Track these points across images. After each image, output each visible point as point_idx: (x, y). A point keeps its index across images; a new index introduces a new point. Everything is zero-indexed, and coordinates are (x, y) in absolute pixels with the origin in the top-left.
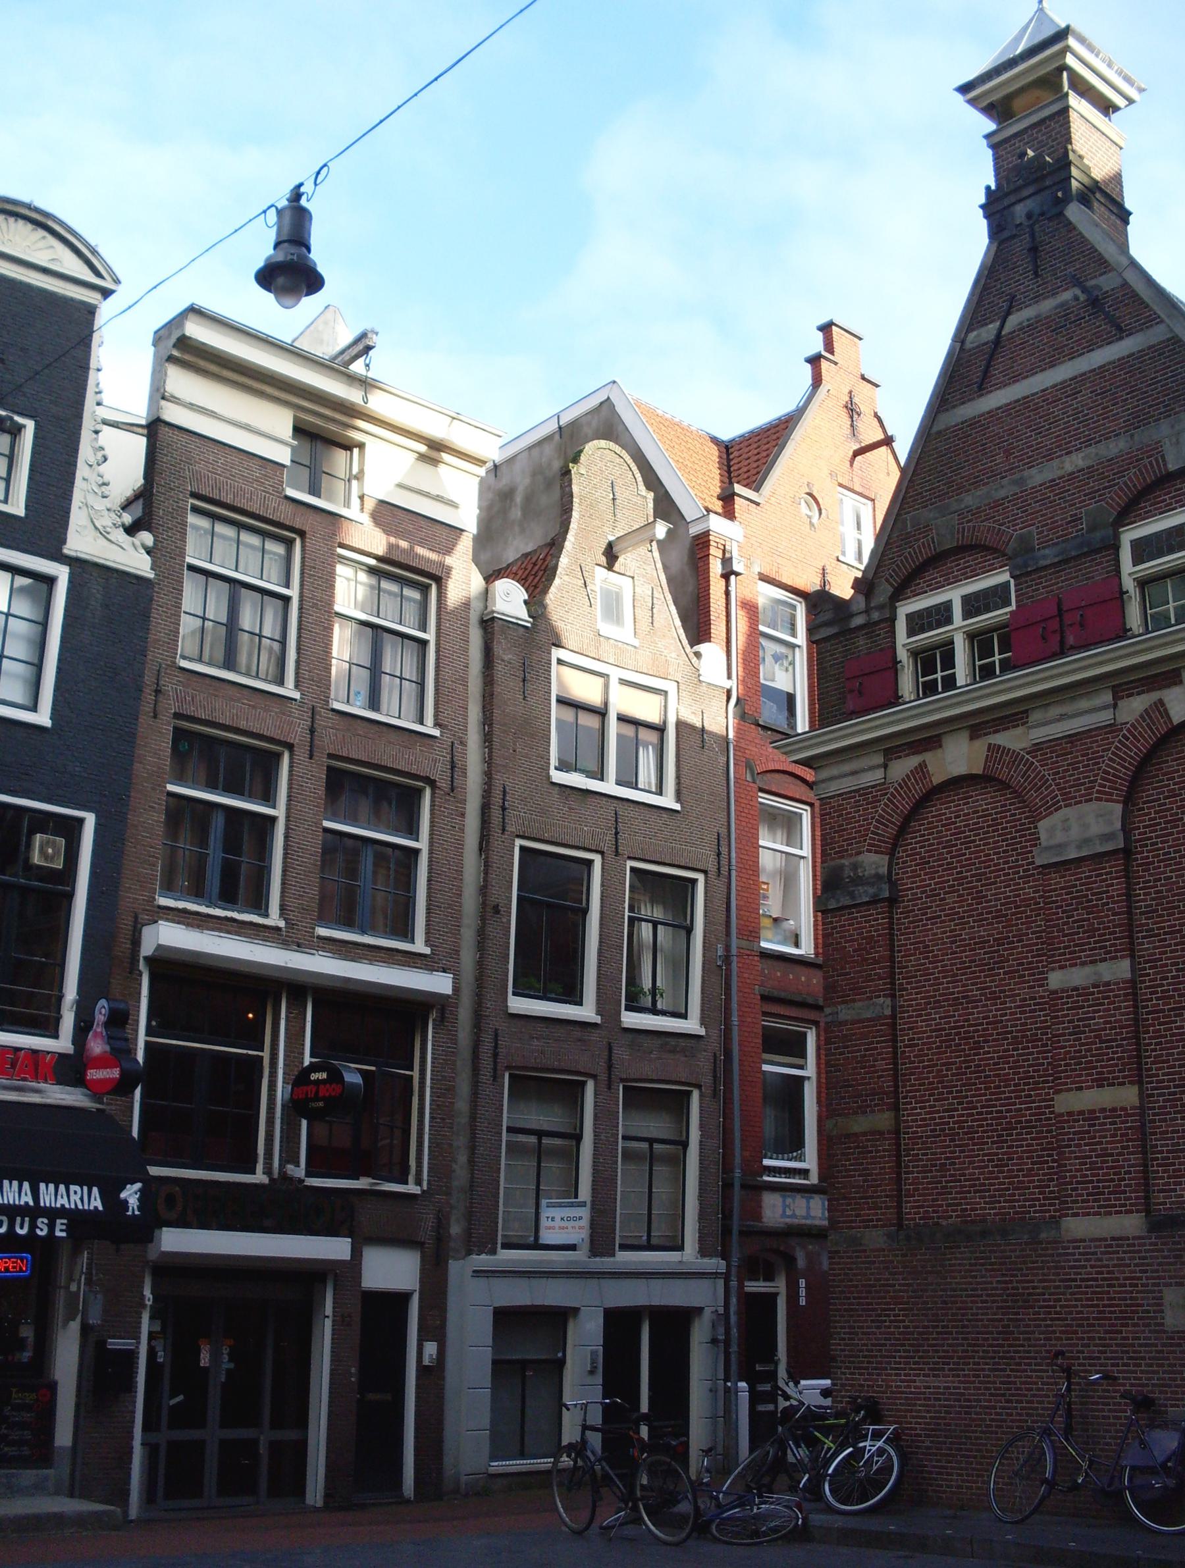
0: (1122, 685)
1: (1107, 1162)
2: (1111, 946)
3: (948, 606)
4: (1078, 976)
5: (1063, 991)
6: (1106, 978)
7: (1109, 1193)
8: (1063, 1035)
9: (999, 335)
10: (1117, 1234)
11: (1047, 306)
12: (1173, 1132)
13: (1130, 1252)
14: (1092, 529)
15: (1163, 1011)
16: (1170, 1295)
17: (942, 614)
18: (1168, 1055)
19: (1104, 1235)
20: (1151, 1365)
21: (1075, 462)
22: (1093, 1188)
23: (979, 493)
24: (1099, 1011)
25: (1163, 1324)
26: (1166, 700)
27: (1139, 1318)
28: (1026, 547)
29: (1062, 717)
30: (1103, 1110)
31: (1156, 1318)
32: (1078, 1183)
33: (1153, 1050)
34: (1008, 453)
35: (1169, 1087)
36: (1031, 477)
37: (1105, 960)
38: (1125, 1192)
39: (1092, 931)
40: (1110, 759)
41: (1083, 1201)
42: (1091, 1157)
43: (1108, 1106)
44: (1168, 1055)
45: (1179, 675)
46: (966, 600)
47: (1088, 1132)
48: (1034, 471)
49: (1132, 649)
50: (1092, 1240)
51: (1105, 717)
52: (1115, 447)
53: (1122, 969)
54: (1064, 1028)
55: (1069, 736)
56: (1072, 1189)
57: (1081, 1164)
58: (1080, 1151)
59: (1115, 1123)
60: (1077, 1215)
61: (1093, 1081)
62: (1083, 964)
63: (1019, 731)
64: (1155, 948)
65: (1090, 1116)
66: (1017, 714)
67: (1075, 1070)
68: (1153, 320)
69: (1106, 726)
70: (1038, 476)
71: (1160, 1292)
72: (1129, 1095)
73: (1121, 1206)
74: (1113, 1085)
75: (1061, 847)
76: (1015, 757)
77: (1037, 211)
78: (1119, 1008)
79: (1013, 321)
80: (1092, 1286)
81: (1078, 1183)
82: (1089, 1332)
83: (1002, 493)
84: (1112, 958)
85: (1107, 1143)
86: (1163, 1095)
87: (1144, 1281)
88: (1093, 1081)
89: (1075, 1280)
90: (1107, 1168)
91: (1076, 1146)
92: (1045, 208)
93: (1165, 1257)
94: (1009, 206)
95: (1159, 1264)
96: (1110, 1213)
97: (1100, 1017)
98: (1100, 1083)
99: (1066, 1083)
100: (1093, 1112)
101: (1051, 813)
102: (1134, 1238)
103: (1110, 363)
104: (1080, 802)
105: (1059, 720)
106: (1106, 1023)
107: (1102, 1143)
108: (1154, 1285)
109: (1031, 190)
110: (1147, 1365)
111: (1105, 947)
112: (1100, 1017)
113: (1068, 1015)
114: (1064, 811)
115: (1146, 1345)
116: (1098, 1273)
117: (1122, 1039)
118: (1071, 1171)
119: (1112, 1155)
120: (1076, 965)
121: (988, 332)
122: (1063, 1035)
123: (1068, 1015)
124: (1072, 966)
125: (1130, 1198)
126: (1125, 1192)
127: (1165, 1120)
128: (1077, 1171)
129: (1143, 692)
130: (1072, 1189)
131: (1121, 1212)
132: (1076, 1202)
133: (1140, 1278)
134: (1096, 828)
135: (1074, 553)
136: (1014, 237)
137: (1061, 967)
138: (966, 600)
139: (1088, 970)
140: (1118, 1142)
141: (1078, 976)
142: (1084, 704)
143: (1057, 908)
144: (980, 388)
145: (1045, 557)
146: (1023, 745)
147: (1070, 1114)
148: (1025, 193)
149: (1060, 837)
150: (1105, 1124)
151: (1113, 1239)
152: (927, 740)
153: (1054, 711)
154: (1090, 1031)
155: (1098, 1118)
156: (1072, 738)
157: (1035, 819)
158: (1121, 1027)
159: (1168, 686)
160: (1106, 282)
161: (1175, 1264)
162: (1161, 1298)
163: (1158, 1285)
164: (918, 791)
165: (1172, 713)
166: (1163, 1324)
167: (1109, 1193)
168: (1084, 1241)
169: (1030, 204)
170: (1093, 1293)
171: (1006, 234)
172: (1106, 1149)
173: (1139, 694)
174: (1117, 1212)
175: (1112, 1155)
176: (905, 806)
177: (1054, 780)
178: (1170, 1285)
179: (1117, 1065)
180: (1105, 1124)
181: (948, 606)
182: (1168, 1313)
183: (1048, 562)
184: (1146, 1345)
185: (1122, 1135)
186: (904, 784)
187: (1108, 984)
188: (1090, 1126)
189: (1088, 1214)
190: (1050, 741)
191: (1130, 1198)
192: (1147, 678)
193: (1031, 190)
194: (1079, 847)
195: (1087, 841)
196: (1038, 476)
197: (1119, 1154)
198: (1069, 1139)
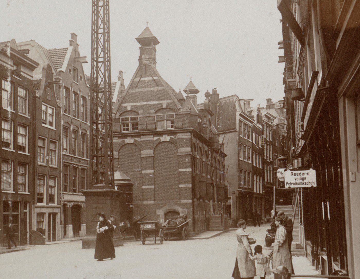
3: (128, 118)
9: (139, 80)
17: (127, 119)
46: (131, 118)
51: (152, 139)
63: (139, 139)
68: (162, 86)
72: (153, 187)
76: (138, 142)
79: (142, 79)
121: (137, 80)
138: (131, 118)
144: (136, 88)
157: (141, 150)
164: (123, 144)
176: (121, 145)
181: (128, 118)
186: (121, 142)
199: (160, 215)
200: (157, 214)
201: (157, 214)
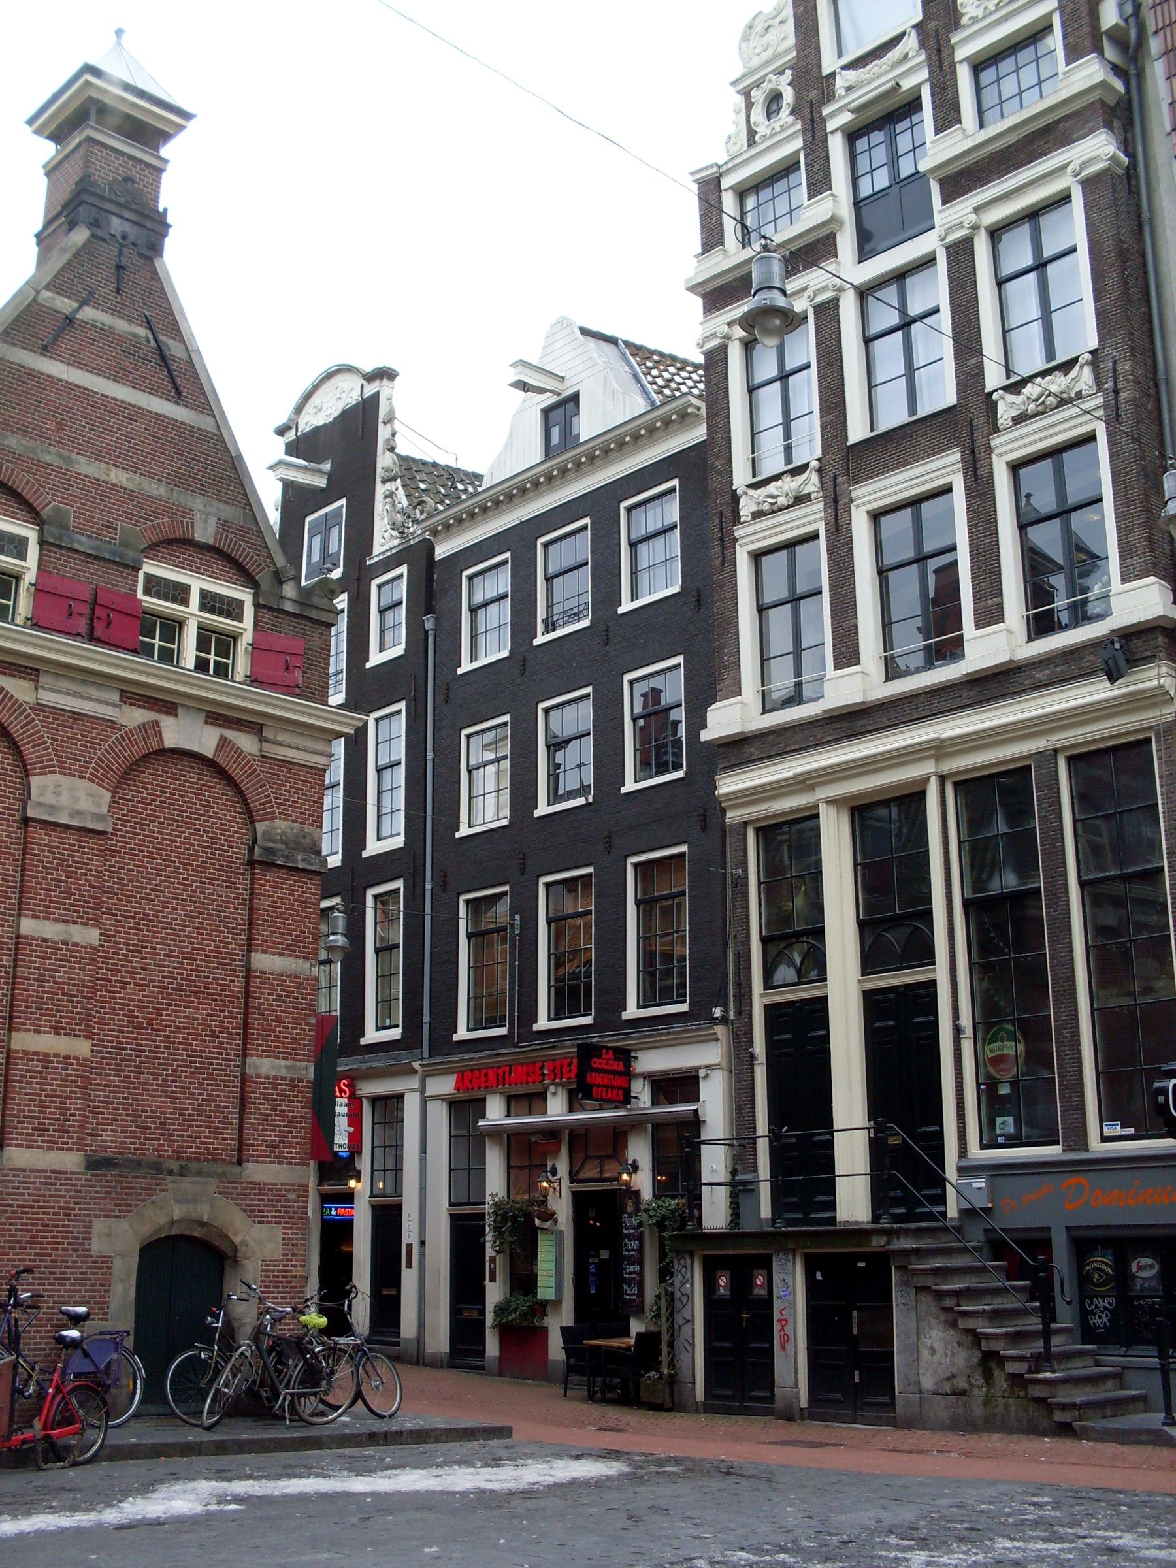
0: (132, 694)
1: (55, 1102)
2: (85, 912)
4: (50, 930)
5: (33, 938)
6: (76, 940)
7: (54, 1131)
8: (29, 979)
10: (57, 1167)
11: (121, 325)
12: (106, 1086)
13: (67, 1185)
14: (125, 544)
15: (111, 981)
16: (99, 1225)
18: (110, 1019)
19: (44, 1168)
20: (75, 1285)
21: (119, 477)
22: (39, 1124)
23: (24, 442)
24: (64, 966)
25: (89, 1250)
26: (162, 724)
27: (69, 1244)
28: (60, 521)
29: (76, 695)
30: (57, 1055)
31: (83, 1244)
32: (25, 1117)
33: (97, 1012)
34: (60, 426)
35: (107, 1047)
36: (77, 462)
37: (75, 923)
38: (68, 1132)
39: (68, 894)
40: (106, 750)
41: (28, 1134)
42: (41, 1095)
43: (63, 1053)
44: (110, 1019)
45: (176, 710)
47: (41, 1072)
48: (82, 459)
49: (156, 672)
50: (32, 1171)
52: (157, 489)
53: (28, 926)
54: (29, 973)
55: (74, 713)
56: (19, 1122)
57: (30, 1100)
58: (31, 1088)
59: (67, 1069)
60: (20, 1146)
61: (51, 1027)
62: (56, 920)
64: (112, 925)
65: (45, 1058)
66: (26, 667)
67: (35, 1014)
69: (108, 720)
70: (85, 466)
71: (91, 1222)
73: (63, 1143)
74: (69, 1035)
75: (53, 808)
77: (131, 238)
78: (84, 969)
79: (88, 313)
80: (28, 1213)
81: (25, 1117)
82: (20, 1254)
83: (48, 458)
84: (82, 924)
85: (58, 1085)
86: (101, 1052)
87: (77, 1211)
88: (51, 1027)
89: (12, 1206)
90: (55, 1108)
91: (27, 1083)
92: (139, 242)
93: (97, 1192)
94: (107, 211)
95: (91, 1198)
96: (52, 1149)
97: (65, 972)
98: (57, 1030)
99: (25, 1024)
100: (47, 1055)
101: (45, 773)
102: (72, 1173)
103: (165, 416)
104: (74, 776)
105: (69, 695)
106: (69, 978)
107: (52, 1085)
108: (85, 1215)
109: (132, 217)
110: (71, 1285)
111: (79, 912)
112: (65, 972)
113: (35, 962)
114: (57, 777)
115: (71, 1267)
116: (34, 1201)
117: (83, 997)
118: (19, 1105)
119: (60, 1097)
120: (48, 919)
122: (29, 979)
123: (35, 962)
124: (44, 918)
125: (72, 1138)
126: (68, 1132)
127: (100, 1074)
128: (25, 1105)
129: (143, 707)
130: (19, 1122)
131: (62, 1149)
132: (22, 1134)
133: (74, 1209)
134: (85, 805)
135: (107, 556)
136: (104, 240)
137: (35, 917)
139: (60, 927)
140: (67, 1086)
141: (50, 930)
142: (93, 692)
143: (38, 861)
145: (79, 542)
146: (27, 699)
147: (26, 1052)
148: (127, 214)
149: (49, 799)
150: (57, 1068)
151: (52, 1172)
152: (167, 705)
153: (65, 684)
154: (55, 982)
155: (52, 1062)
156: (76, 716)
158: (84, 986)
159: (167, 713)
160: (174, 349)
161: (105, 1198)
162: (90, 1227)
163: (89, 1215)
165: (165, 736)
166: (89, 1250)
167: (54, 1131)
168: (24, 1170)
169: (127, 227)
170: (28, 1219)
171: (99, 232)
172: (56, 1091)
173: (140, 706)
174: (58, 1149)
175: (60, 1097)
177: (52, 744)
178: (99, 1216)
179: (75, 1018)
180: (57, 1068)
182: (95, 1239)
183: (83, 550)
184: (71, 1267)
185: (72, 1081)
187: (76, 945)
188: (43, 1067)
189: (32, 1147)
190: (54, 708)
191: (72, 1138)
192: (149, 697)
193: (132, 217)
194: (71, 816)
195: (79, 813)
196: (85, 466)
197: (66, 1097)
198: (22, 1076)
199: (117, 1263)
200: (98, 1246)
201: (98, 1246)
